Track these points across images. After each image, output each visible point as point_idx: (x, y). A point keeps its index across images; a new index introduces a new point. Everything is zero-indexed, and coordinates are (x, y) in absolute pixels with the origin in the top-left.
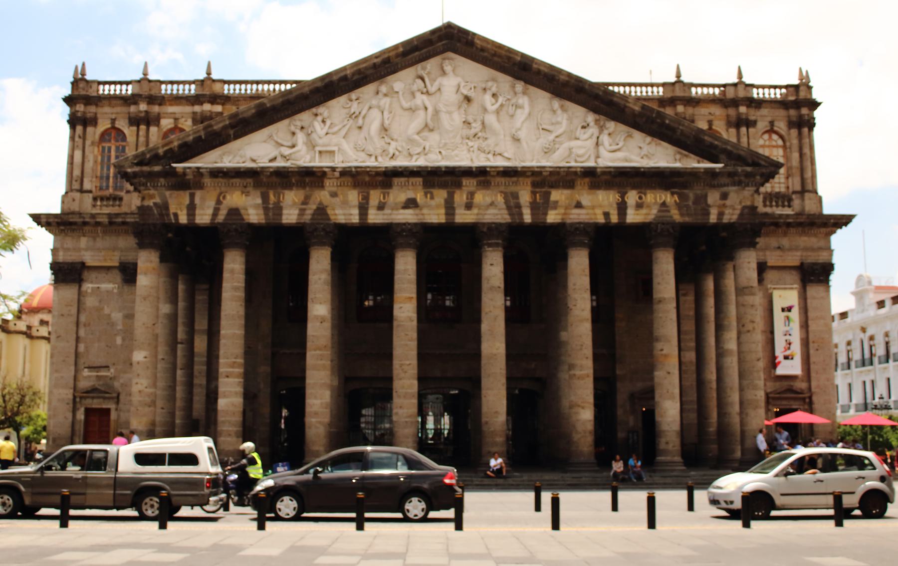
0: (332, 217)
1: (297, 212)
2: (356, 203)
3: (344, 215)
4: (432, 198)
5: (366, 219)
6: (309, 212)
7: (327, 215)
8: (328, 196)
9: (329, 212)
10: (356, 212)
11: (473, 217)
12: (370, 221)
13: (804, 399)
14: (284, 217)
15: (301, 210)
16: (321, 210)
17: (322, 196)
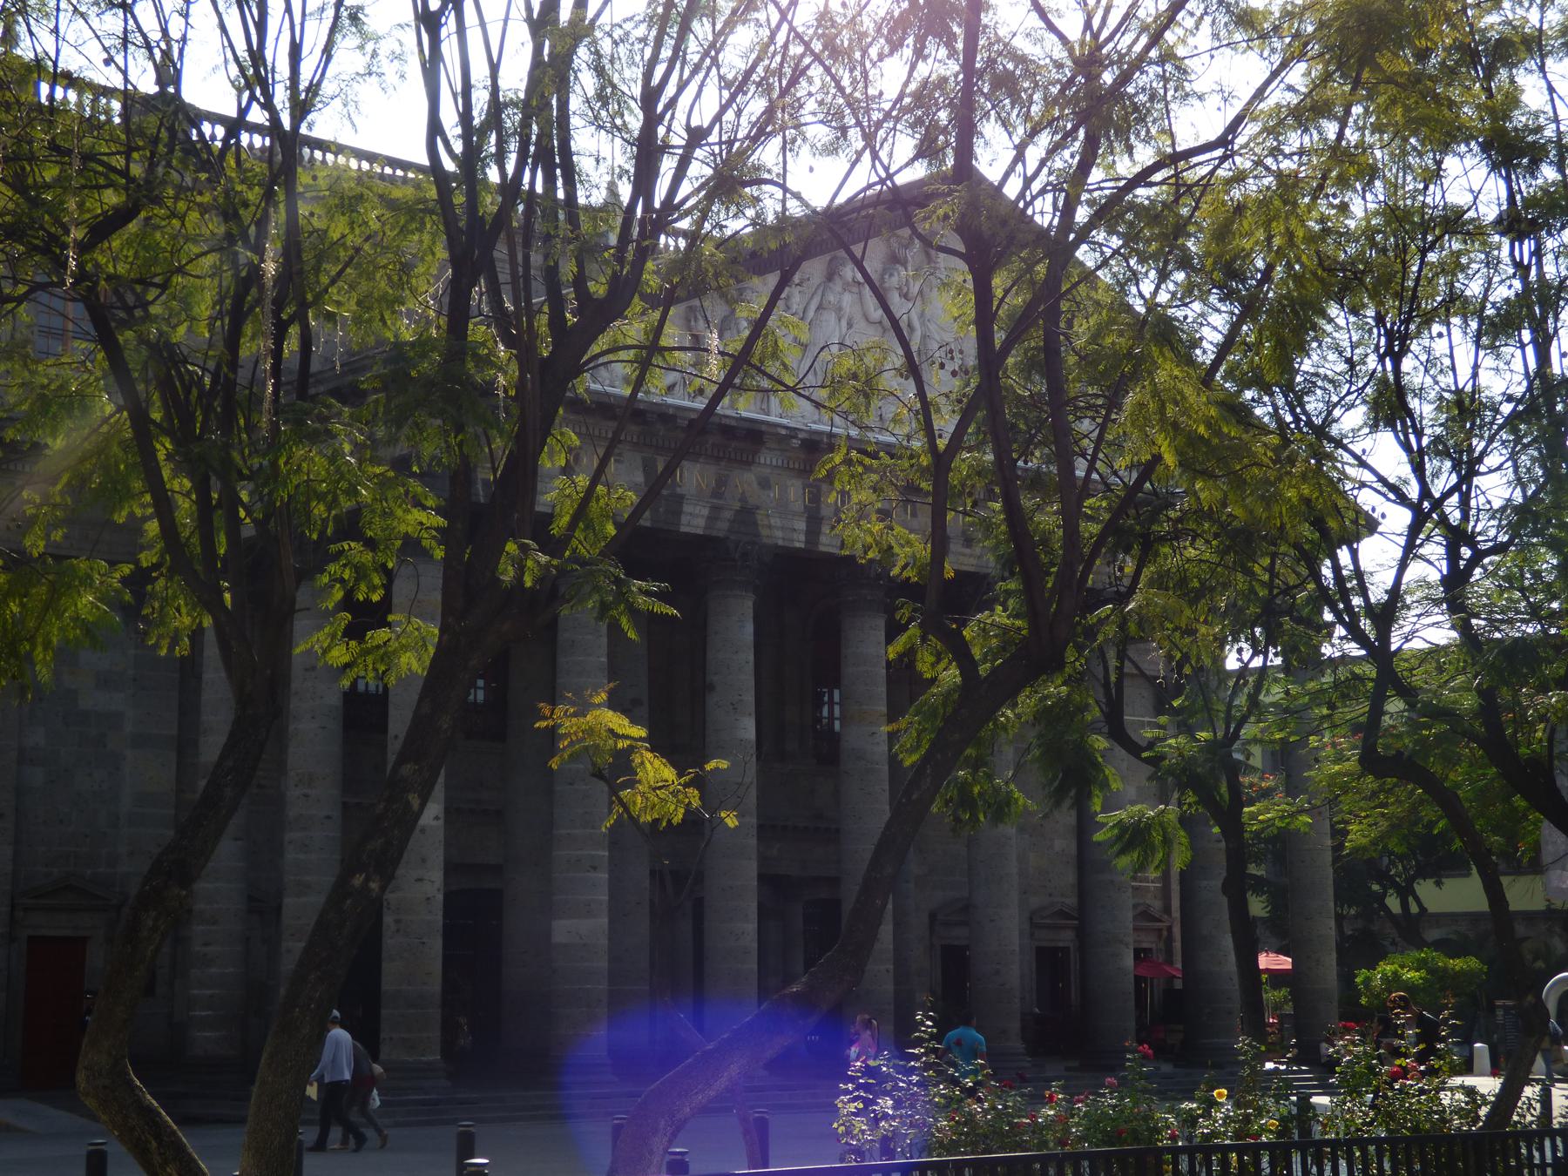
0: (764, 532)
1: (706, 512)
2: (798, 506)
3: (782, 528)
4: (914, 515)
5: (817, 544)
6: (728, 514)
7: (755, 524)
8: (755, 485)
9: (760, 517)
10: (801, 525)
11: (973, 561)
12: (822, 549)
13: (1160, 930)
14: (684, 519)
15: (716, 509)
16: (747, 514)
17: (745, 481)
